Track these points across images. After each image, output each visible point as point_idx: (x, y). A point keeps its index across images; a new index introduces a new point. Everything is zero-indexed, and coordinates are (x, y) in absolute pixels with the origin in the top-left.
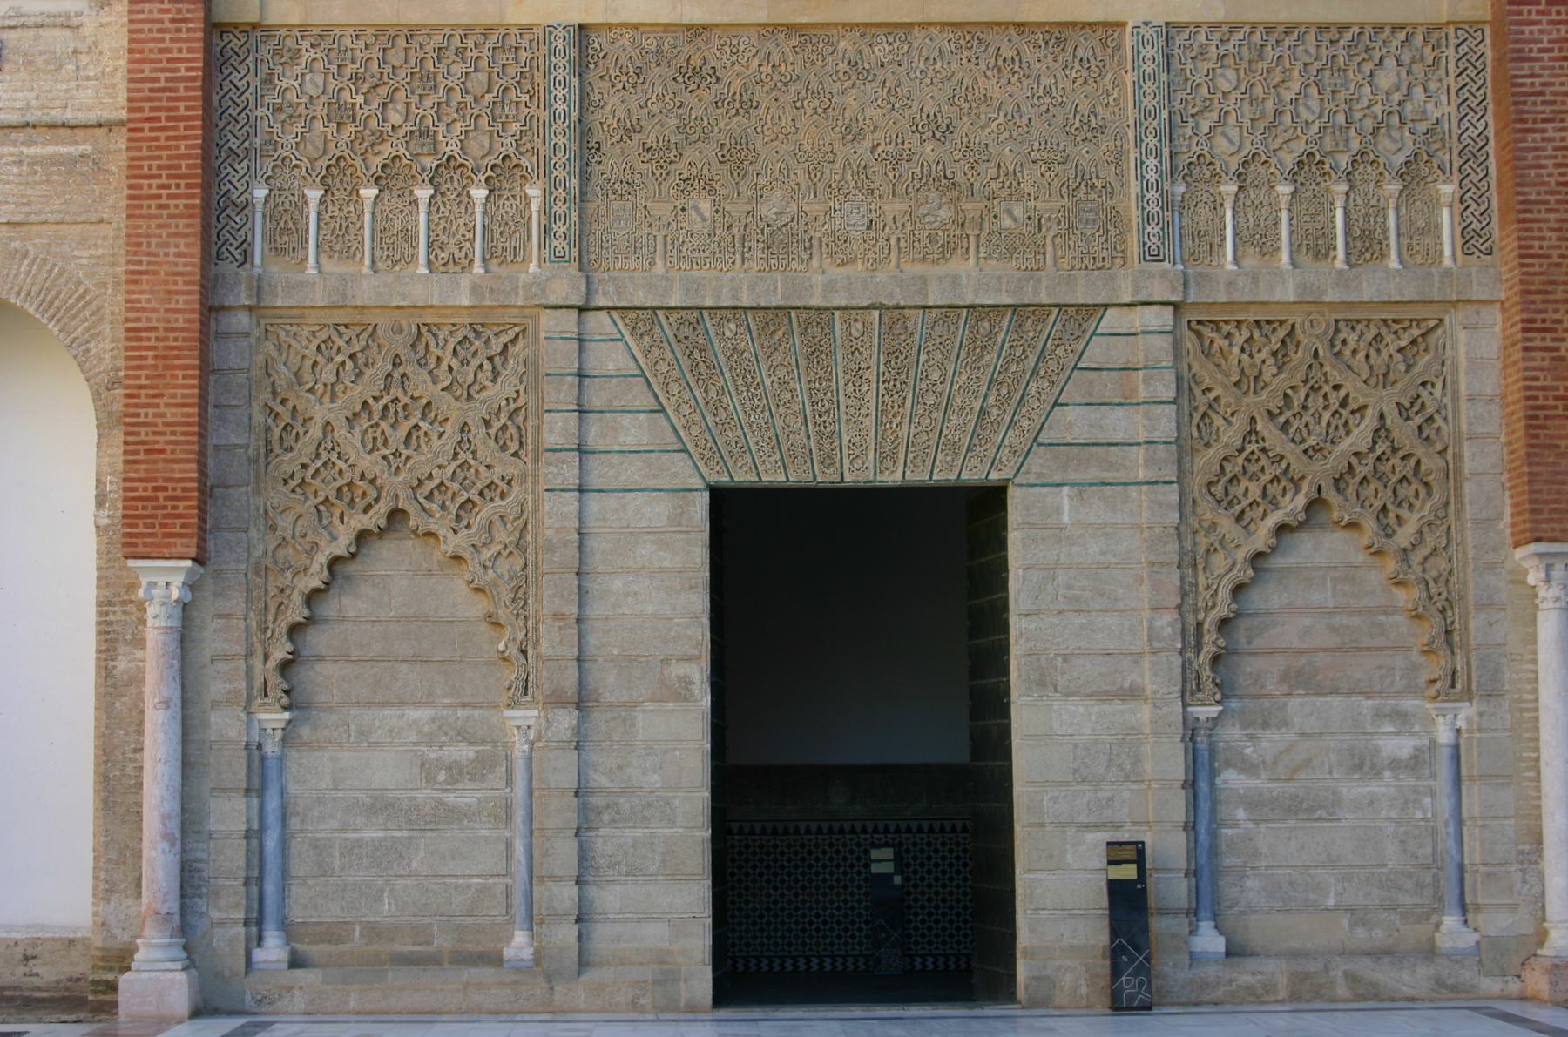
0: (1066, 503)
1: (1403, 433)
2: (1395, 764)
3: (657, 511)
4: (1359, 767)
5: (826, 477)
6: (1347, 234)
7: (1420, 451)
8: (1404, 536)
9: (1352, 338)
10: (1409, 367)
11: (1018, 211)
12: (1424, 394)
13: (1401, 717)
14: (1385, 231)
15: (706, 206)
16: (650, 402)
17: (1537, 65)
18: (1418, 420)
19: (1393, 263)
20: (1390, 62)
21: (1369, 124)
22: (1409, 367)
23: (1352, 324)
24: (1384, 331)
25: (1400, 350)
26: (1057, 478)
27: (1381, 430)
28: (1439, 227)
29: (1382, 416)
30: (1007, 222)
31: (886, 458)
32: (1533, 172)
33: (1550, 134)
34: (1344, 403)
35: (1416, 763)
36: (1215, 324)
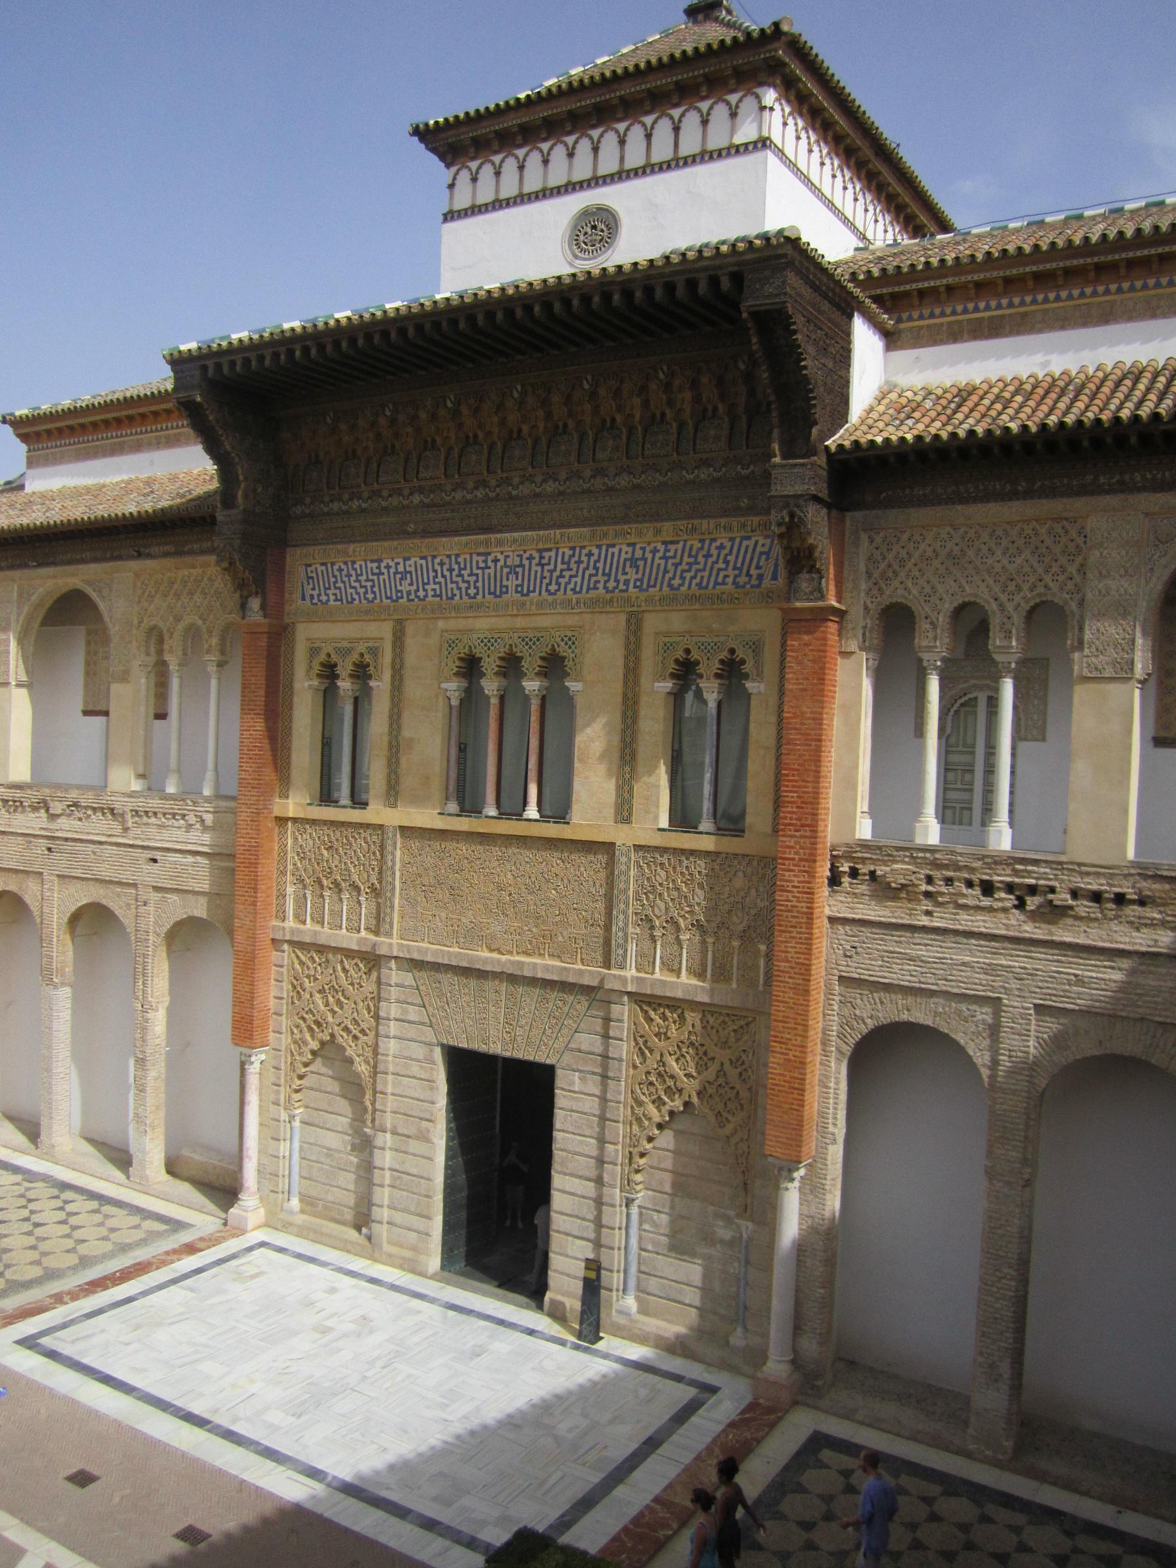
0: (577, 1079)
1: (732, 1073)
2: (722, 1241)
3: (418, 1051)
4: (705, 1239)
5: (483, 1048)
6: (714, 964)
7: (738, 1087)
8: (729, 1128)
9: (711, 1020)
10: (738, 1040)
11: (565, 933)
12: (744, 1057)
13: (728, 1220)
14: (732, 966)
15: (443, 915)
16: (419, 1001)
17: (790, 895)
18: (739, 1070)
19: (734, 986)
20: (740, 874)
21: (727, 907)
22: (738, 1040)
23: (712, 1013)
24: (727, 1019)
25: (734, 1031)
26: (575, 1067)
27: (721, 1072)
28: (758, 967)
29: (722, 1064)
30: (560, 939)
31: (505, 1043)
32: (783, 955)
33: (794, 935)
34: (705, 1053)
35: (731, 1243)
36: (649, 1004)
